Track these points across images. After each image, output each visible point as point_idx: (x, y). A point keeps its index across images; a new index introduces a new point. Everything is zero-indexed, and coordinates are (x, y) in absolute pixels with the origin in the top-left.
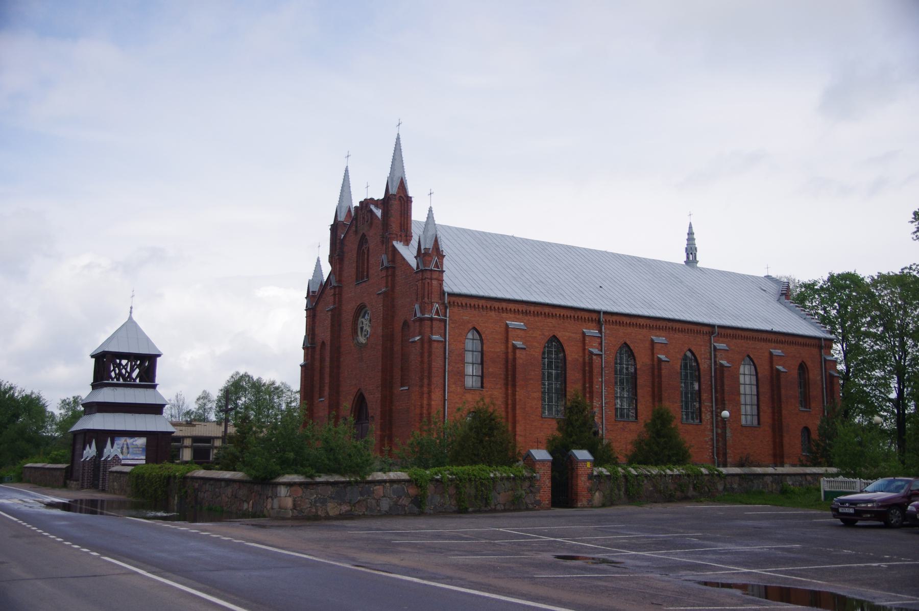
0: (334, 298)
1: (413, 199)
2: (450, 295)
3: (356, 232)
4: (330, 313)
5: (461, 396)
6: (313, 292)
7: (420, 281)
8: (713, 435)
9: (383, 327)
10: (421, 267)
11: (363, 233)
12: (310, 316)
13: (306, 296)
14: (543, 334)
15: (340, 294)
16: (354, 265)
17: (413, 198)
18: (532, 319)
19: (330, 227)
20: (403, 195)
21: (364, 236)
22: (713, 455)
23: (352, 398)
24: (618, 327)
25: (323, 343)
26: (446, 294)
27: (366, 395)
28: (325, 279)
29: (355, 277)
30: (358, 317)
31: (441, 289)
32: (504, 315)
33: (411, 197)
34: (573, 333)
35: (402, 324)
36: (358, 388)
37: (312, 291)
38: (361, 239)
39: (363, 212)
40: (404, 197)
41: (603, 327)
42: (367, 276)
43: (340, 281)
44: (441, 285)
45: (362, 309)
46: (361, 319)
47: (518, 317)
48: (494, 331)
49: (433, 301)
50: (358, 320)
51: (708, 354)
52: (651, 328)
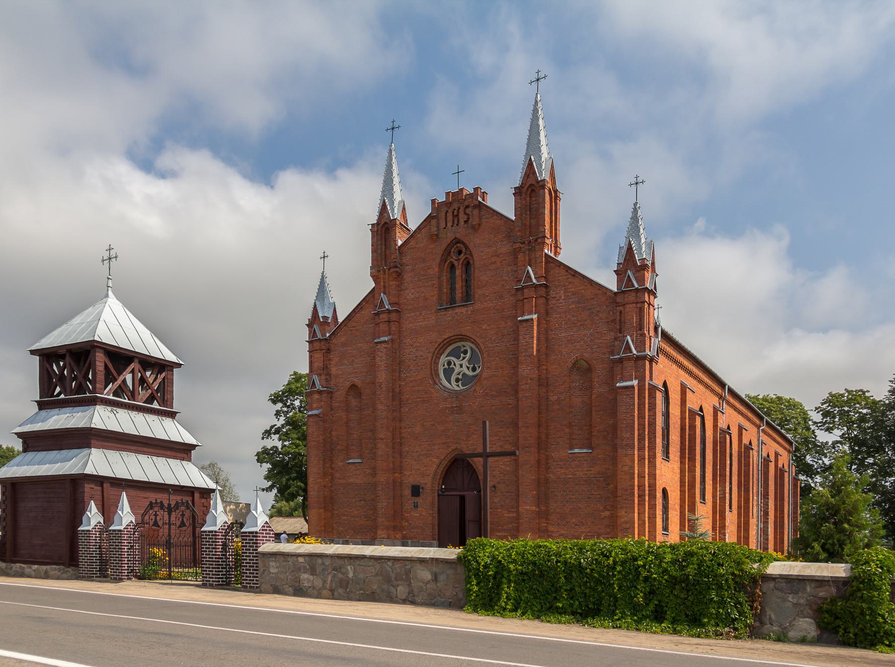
30: (441, 355)
35: (570, 365)
37: (322, 317)
42: (468, 297)
45: (450, 345)
50: (439, 358)
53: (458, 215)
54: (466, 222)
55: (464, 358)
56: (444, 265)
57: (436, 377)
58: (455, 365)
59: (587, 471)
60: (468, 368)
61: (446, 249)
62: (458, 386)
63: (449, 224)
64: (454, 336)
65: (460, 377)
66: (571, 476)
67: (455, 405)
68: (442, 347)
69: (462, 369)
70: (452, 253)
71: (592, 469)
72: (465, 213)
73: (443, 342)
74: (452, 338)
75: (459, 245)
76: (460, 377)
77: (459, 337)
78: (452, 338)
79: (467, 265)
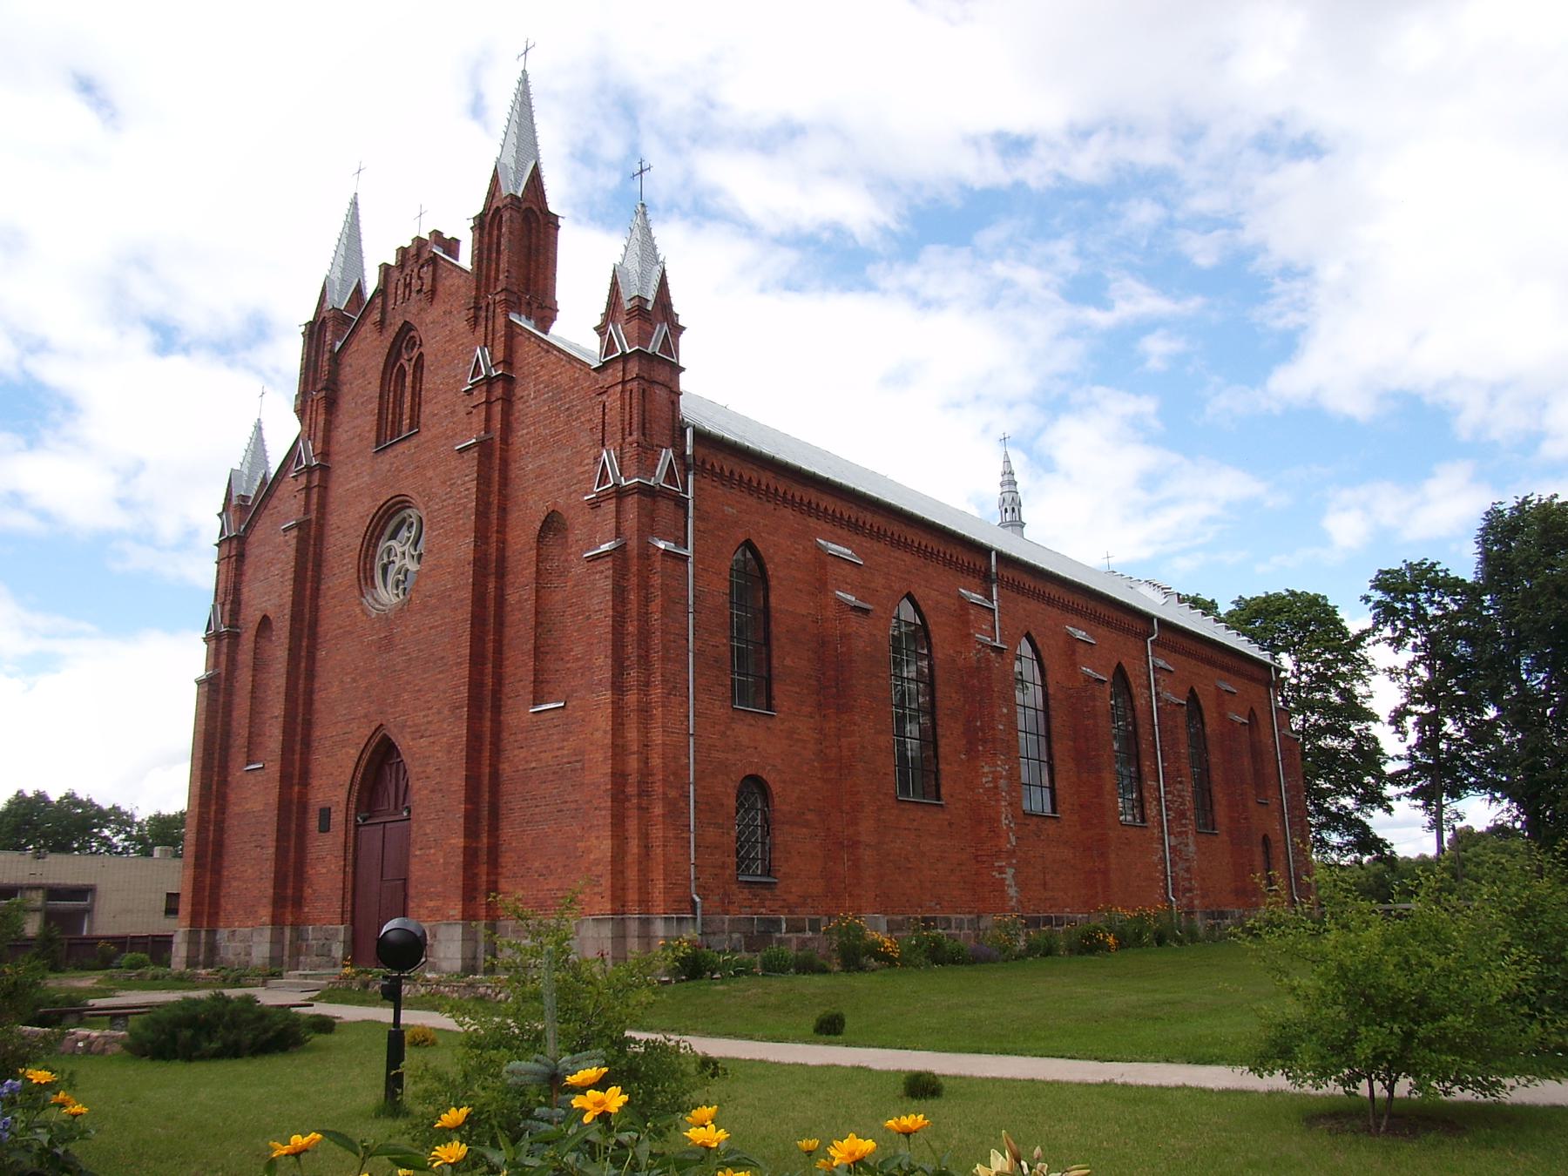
0: (308, 497)
1: (561, 222)
2: (702, 437)
3: (381, 325)
4: (294, 533)
5: (722, 728)
6: (244, 498)
7: (620, 387)
8: (1164, 851)
9: (475, 537)
10: (624, 346)
11: (407, 327)
12: (229, 557)
13: (220, 510)
14: (890, 588)
15: (324, 487)
16: (375, 405)
17: (560, 219)
18: (869, 545)
19: (303, 329)
20: (535, 208)
21: (407, 327)
22: (1167, 895)
23: (354, 753)
24: (1014, 595)
25: (265, 622)
26: (689, 432)
27: (403, 742)
28: (274, 467)
29: (373, 435)
30: (379, 538)
31: (674, 416)
32: (812, 522)
33: (556, 217)
34: (942, 594)
35: (538, 525)
36: (377, 724)
38: (395, 340)
39: (408, 271)
40: (538, 213)
41: (994, 590)
42: (415, 422)
43: (325, 454)
44: (674, 404)
45: (391, 517)
46: (384, 544)
47: (839, 531)
48: (793, 558)
49: (656, 442)
50: (376, 546)
51: (1145, 677)
52: (1065, 607)
53: (410, 283)
54: (419, 291)
55: (409, 538)
56: (392, 372)
57: (366, 584)
58: (396, 555)
59: (558, 749)
60: (413, 556)
61: (393, 344)
62: (398, 595)
63: (399, 298)
64: (392, 498)
65: (401, 577)
66: (533, 765)
67: (383, 635)
68: (377, 524)
69: (403, 562)
70: (403, 350)
71: (565, 743)
72: (420, 278)
73: (377, 512)
74: (390, 503)
75: (412, 334)
76: (401, 577)
77: (398, 499)
78: (390, 503)
79: (419, 364)
